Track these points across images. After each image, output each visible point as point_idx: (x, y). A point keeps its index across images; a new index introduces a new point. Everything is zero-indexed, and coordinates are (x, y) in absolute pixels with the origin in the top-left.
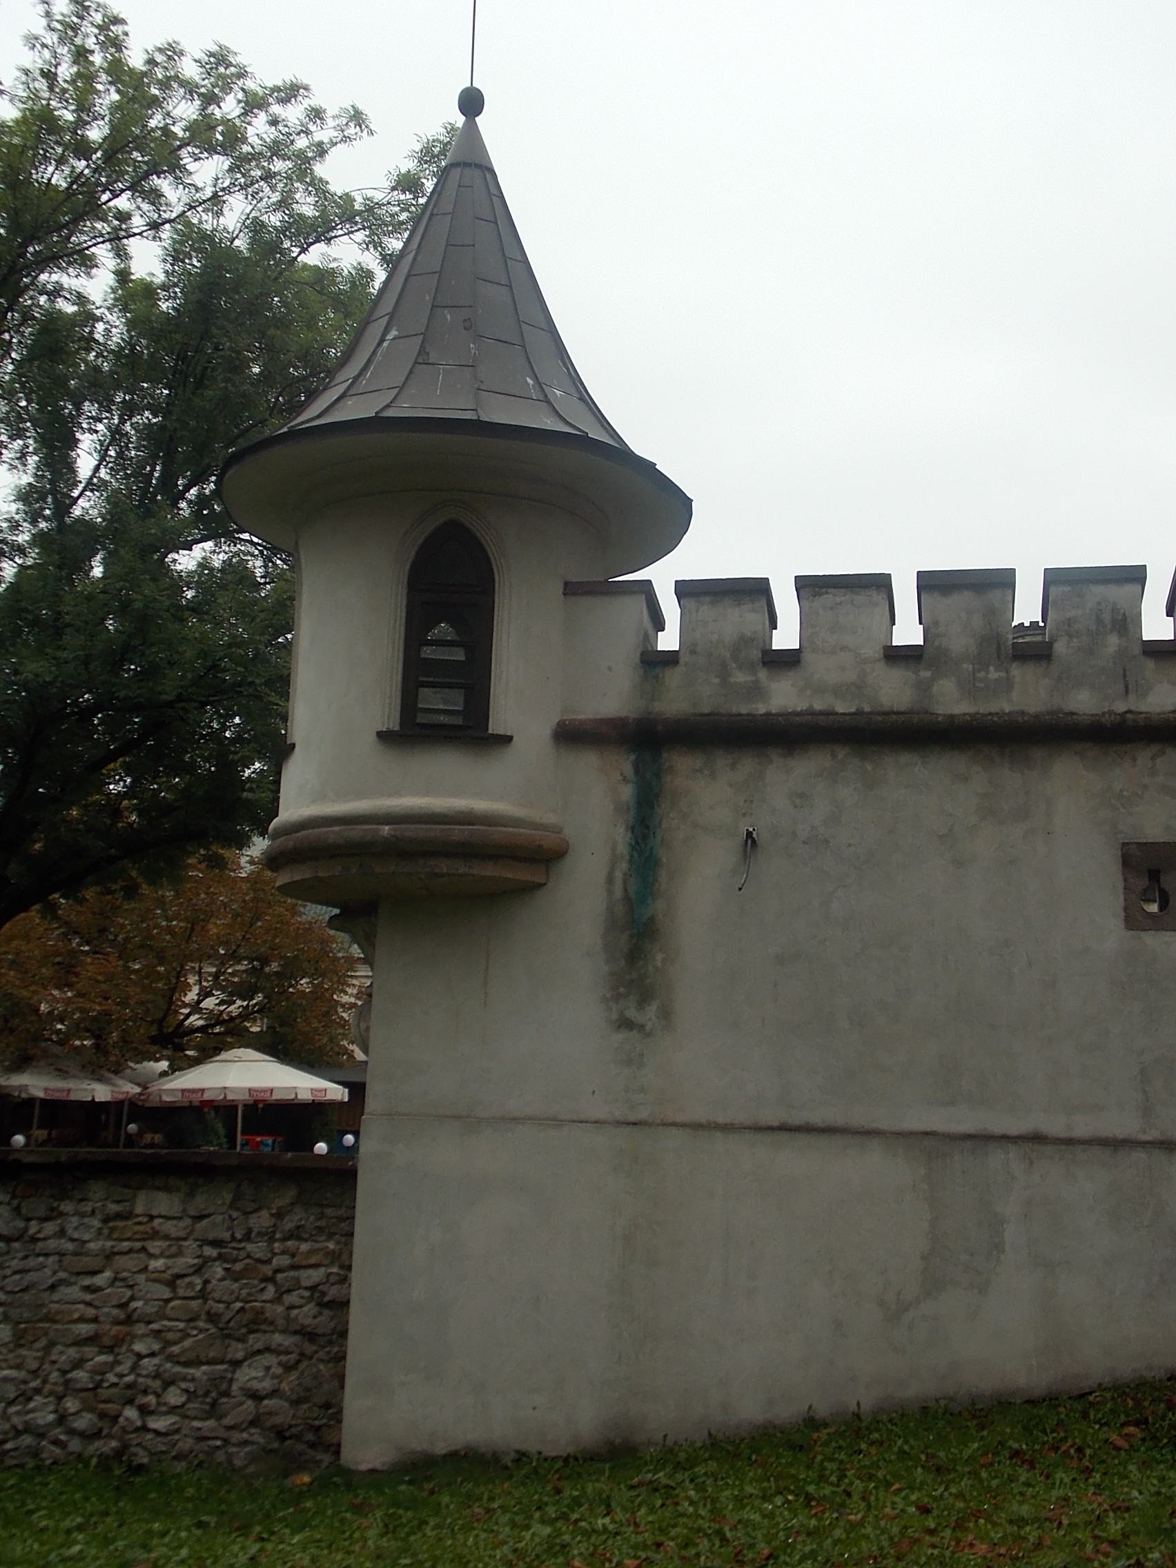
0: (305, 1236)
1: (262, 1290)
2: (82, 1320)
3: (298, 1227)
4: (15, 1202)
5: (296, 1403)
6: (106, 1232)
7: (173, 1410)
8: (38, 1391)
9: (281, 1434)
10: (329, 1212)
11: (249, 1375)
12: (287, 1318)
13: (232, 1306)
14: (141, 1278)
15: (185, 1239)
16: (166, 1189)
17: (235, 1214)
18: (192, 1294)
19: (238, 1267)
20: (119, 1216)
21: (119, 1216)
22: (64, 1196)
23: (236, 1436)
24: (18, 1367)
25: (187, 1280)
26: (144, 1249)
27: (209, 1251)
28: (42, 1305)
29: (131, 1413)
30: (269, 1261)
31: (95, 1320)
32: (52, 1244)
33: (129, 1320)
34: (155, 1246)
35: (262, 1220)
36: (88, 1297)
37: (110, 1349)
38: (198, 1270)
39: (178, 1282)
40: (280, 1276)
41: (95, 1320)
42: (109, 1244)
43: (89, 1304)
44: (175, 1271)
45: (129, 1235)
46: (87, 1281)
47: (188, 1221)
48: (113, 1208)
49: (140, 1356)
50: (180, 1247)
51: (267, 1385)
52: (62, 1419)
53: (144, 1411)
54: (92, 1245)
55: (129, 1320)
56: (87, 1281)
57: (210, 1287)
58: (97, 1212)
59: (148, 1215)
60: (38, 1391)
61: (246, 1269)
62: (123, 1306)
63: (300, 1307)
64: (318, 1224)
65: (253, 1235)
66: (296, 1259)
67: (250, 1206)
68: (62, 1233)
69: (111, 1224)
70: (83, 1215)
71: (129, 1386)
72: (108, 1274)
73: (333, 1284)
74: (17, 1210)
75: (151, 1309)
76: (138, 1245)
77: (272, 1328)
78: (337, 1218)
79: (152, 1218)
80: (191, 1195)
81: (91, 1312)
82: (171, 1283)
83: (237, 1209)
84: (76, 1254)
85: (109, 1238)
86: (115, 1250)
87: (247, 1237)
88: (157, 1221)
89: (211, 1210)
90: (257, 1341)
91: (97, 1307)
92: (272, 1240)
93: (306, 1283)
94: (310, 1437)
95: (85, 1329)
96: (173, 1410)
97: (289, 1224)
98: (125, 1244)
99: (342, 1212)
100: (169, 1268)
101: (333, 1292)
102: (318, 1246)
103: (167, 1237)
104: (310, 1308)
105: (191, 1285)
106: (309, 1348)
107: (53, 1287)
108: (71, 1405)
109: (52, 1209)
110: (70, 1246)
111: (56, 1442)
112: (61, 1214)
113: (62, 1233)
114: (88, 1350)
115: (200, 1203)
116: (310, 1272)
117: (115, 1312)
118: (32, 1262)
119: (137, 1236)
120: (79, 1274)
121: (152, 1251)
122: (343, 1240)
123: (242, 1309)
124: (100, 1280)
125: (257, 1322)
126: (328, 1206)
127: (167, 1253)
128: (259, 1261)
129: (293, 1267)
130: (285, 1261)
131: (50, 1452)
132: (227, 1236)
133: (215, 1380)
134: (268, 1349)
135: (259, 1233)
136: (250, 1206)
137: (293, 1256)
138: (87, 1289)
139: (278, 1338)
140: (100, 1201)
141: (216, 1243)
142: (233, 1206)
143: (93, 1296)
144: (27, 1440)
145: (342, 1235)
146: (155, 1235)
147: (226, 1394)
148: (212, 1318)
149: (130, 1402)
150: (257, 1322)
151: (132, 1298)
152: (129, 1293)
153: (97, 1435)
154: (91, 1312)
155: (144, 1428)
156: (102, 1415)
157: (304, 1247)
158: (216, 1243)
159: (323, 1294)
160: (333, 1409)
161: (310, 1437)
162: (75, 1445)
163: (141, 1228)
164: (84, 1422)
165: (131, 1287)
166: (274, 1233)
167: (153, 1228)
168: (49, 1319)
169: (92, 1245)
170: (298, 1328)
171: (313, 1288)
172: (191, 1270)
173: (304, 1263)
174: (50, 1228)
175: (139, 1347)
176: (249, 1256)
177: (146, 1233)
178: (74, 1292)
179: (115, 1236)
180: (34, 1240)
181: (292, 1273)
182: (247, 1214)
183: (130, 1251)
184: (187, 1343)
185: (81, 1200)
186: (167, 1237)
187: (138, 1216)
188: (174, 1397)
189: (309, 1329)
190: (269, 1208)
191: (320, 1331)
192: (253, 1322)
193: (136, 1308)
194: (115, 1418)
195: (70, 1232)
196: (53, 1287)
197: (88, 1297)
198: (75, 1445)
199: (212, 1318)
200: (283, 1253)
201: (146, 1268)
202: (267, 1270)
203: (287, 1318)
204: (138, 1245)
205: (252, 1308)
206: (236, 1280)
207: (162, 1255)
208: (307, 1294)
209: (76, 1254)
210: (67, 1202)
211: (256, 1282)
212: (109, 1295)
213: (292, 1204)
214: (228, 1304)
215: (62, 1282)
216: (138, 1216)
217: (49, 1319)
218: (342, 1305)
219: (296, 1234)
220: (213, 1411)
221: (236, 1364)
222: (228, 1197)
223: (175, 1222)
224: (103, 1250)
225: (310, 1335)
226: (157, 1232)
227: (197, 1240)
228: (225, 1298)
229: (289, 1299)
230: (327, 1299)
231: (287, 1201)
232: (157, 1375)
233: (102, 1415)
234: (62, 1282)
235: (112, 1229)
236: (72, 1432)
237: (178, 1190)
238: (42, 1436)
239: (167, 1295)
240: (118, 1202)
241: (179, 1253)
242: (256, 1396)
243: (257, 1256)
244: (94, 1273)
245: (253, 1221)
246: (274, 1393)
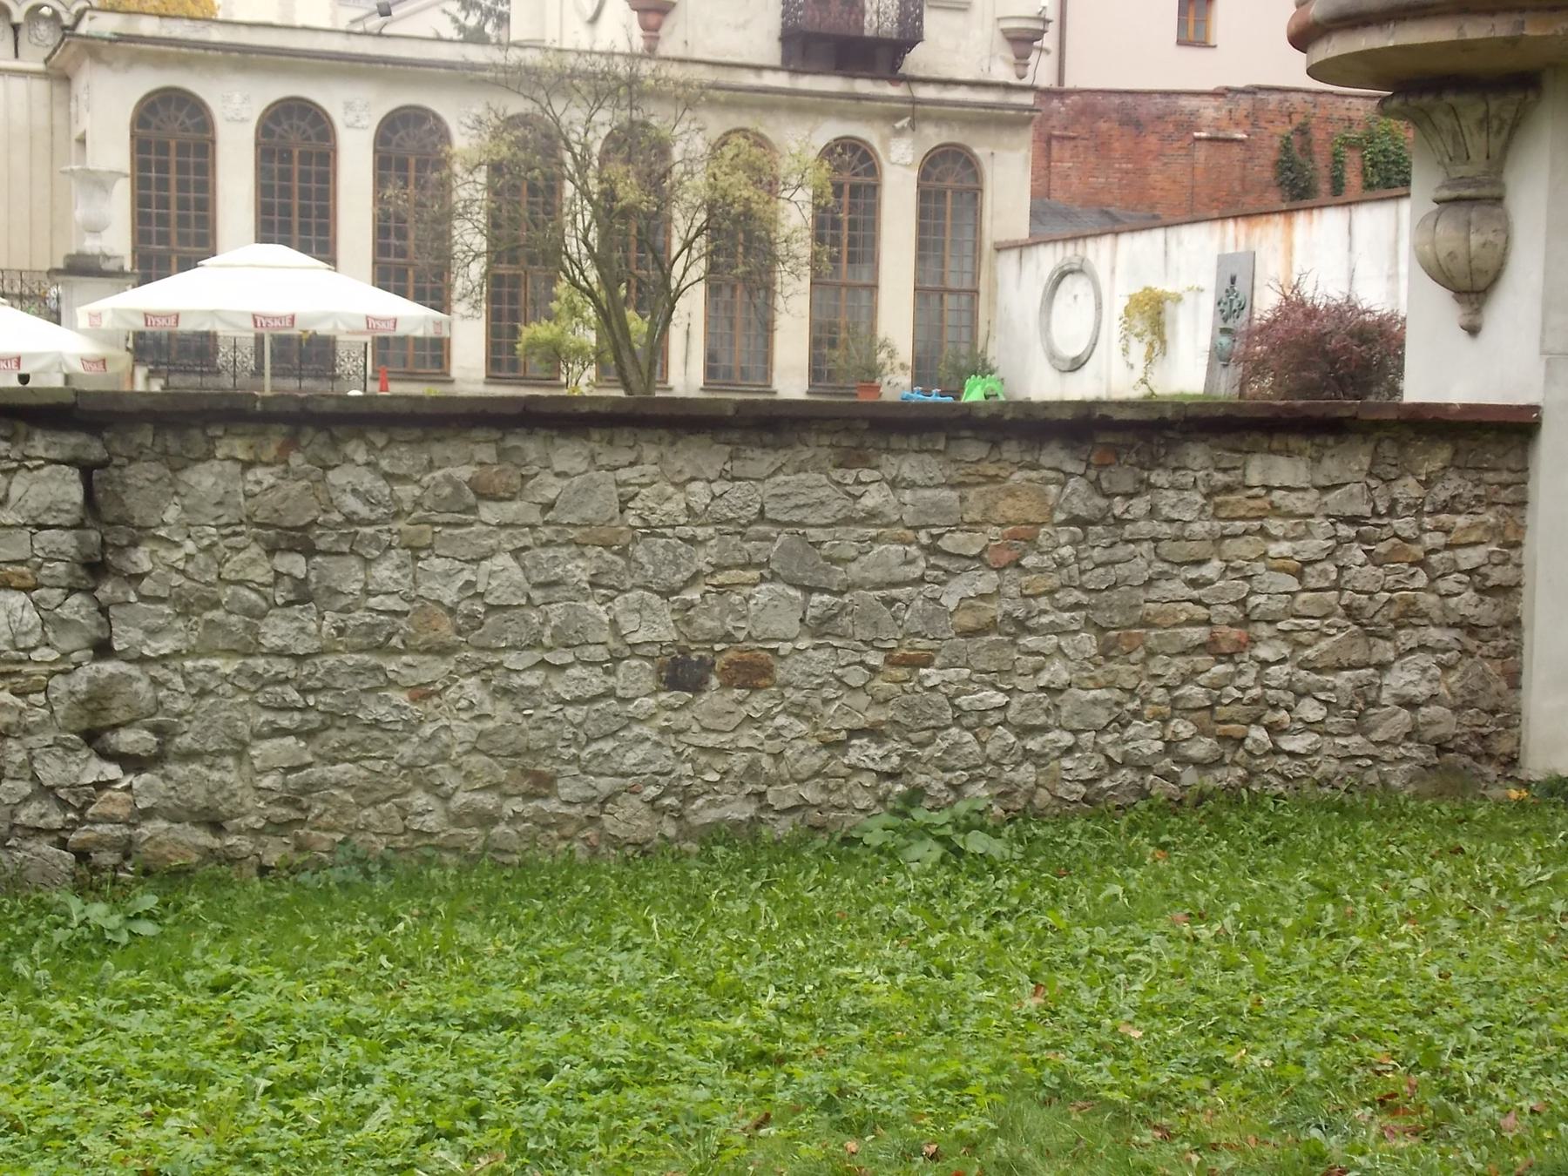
0: (1461, 507)
1: (1413, 575)
2: (1191, 622)
3: (1453, 497)
4: (1092, 474)
5: (1455, 709)
6: (1210, 509)
7: (1309, 726)
8: (1137, 714)
9: (1441, 748)
10: (1489, 477)
11: (1404, 679)
12: (1444, 609)
13: (1376, 597)
14: (1260, 567)
15: (1312, 516)
16: (1289, 453)
17: (1373, 483)
18: (1327, 584)
19: (1381, 548)
20: (1228, 489)
21: (1228, 489)
22: (1155, 464)
23: (1389, 753)
24: (1109, 686)
25: (1319, 566)
26: (1263, 531)
27: (1345, 530)
28: (1138, 606)
29: (1258, 733)
30: (1417, 541)
31: (1208, 622)
32: (1144, 527)
33: (1247, 620)
34: (1275, 526)
35: (1407, 489)
36: (1195, 594)
37: (1230, 656)
38: (1331, 555)
39: (1308, 570)
40: (1434, 558)
41: (1208, 622)
42: (1217, 525)
43: (1197, 602)
44: (1305, 556)
45: (1242, 513)
46: (1193, 573)
47: (1314, 494)
48: (1220, 478)
49: (1265, 664)
50: (1307, 525)
51: (1423, 690)
52: (1170, 746)
53: (1274, 729)
54: (1196, 527)
55: (1247, 620)
56: (1193, 573)
57: (1347, 575)
58: (1200, 483)
59: (1264, 486)
60: (1137, 714)
61: (1393, 550)
62: (1242, 603)
63: (1459, 594)
64: (1477, 492)
65: (1399, 508)
66: (1452, 536)
67: (1393, 473)
68: (1153, 512)
69: (1218, 499)
70: (1181, 489)
71: (1255, 701)
72: (1217, 564)
73: (1496, 565)
74: (1095, 485)
75: (1278, 604)
76: (1256, 524)
77: (1426, 621)
78: (1499, 484)
79: (1269, 489)
80: (1317, 460)
81: (1201, 612)
82: (1299, 574)
83: (1378, 477)
84: (1176, 539)
85: (1215, 516)
86: (1226, 532)
87: (1391, 512)
88: (1277, 496)
89: (1348, 477)
90: (1407, 637)
91: (1207, 606)
92: (1419, 513)
93: (1465, 566)
94: (1475, 747)
95: (1198, 634)
96: (1309, 726)
97: (1442, 493)
98: (1238, 523)
99: (1506, 477)
100: (1296, 553)
101: (1497, 576)
102: (1477, 519)
103: (1290, 514)
104: (1469, 595)
105: (1324, 573)
106: (1472, 644)
107: (1149, 583)
108: (1182, 728)
109: (1141, 482)
110: (1166, 529)
111: (1167, 776)
112: (1151, 486)
113: (1153, 512)
114: (1201, 661)
115: (1331, 468)
116: (1470, 552)
117: (1233, 610)
118: (1121, 551)
119: (1252, 514)
120: (1181, 564)
121: (1274, 532)
122: (1508, 510)
123: (1390, 601)
124: (1211, 570)
125: (1410, 615)
126: (1487, 470)
127: (1292, 535)
128: (1406, 540)
129: (1448, 547)
130: (1439, 539)
131: (1161, 789)
132: (1366, 510)
133: (1360, 689)
134: (1422, 647)
135: (1408, 507)
136: (1393, 473)
137: (1448, 532)
138: (1193, 583)
139: (1434, 635)
140: (1202, 468)
141: (1352, 520)
142: (1370, 474)
143: (1202, 591)
144: (1126, 776)
145: (1507, 505)
146: (1275, 510)
147: (1374, 704)
148: (1351, 612)
149: (1256, 720)
150: (1410, 615)
151: (1252, 592)
152: (1247, 587)
153: (1218, 762)
154: (1201, 612)
155: (1277, 751)
156: (1222, 739)
157: (1461, 521)
158: (1352, 520)
159: (1486, 577)
160: (1509, 717)
161: (1475, 747)
162: (1189, 776)
163: (1258, 503)
164: (1201, 749)
165: (1248, 578)
166: (1423, 504)
167: (1271, 503)
168: (1146, 624)
169: (1196, 527)
170: (1458, 619)
171: (1470, 572)
172: (1324, 555)
173: (1463, 541)
174: (1140, 506)
175: (1264, 652)
176: (1396, 535)
177: (1263, 509)
178: (1178, 588)
179: (1223, 514)
180: (1120, 522)
181: (1447, 554)
182: (1387, 481)
183: (1246, 533)
184: (1324, 644)
185: (1175, 469)
186: (1290, 514)
187: (1251, 487)
188: (1311, 710)
189: (1472, 621)
190: (1413, 474)
191: (1483, 622)
192: (1403, 615)
193: (1257, 606)
194: (1241, 741)
195: (1166, 511)
196: (1149, 583)
197: (1195, 594)
198: (1189, 776)
199: (1351, 612)
200: (1436, 529)
201: (1266, 553)
202: (1417, 551)
203: (1444, 609)
204: (1256, 524)
205: (1401, 598)
206: (1380, 566)
207: (1285, 538)
208: (1466, 578)
209: (1176, 539)
210: (1160, 471)
211: (1405, 566)
212: (1223, 588)
213: (1444, 468)
214: (1371, 594)
215: (1163, 575)
216: (1251, 487)
217: (1146, 624)
218: (1508, 590)
219: (1449, 507)
220: (1359, 725)
221: (1383, 667)
222: (1366, 461)
223: (1300, 495)
224: (1210, 532)
225: (1472, 629)
226: (1279, 508)
227: (1328, 516)
228: (1368, 588)
229: (1445, 585)
230: (1489, 583)
231: (1440, 464)
232: (1289, 687)
233: (1222, 739)
234: (1163, 575)
235: (1218, 506)
236: (1185, 761)
237: (1301, 453)
238: (1147, 768)
239: (1296, 587)
240: (1225, 470)
241: (1308, 533)
242: (1411, 704)
243: (1405, 534)
244: (1199, 563)
245: (1397, 490)
246: (1434, 698)
